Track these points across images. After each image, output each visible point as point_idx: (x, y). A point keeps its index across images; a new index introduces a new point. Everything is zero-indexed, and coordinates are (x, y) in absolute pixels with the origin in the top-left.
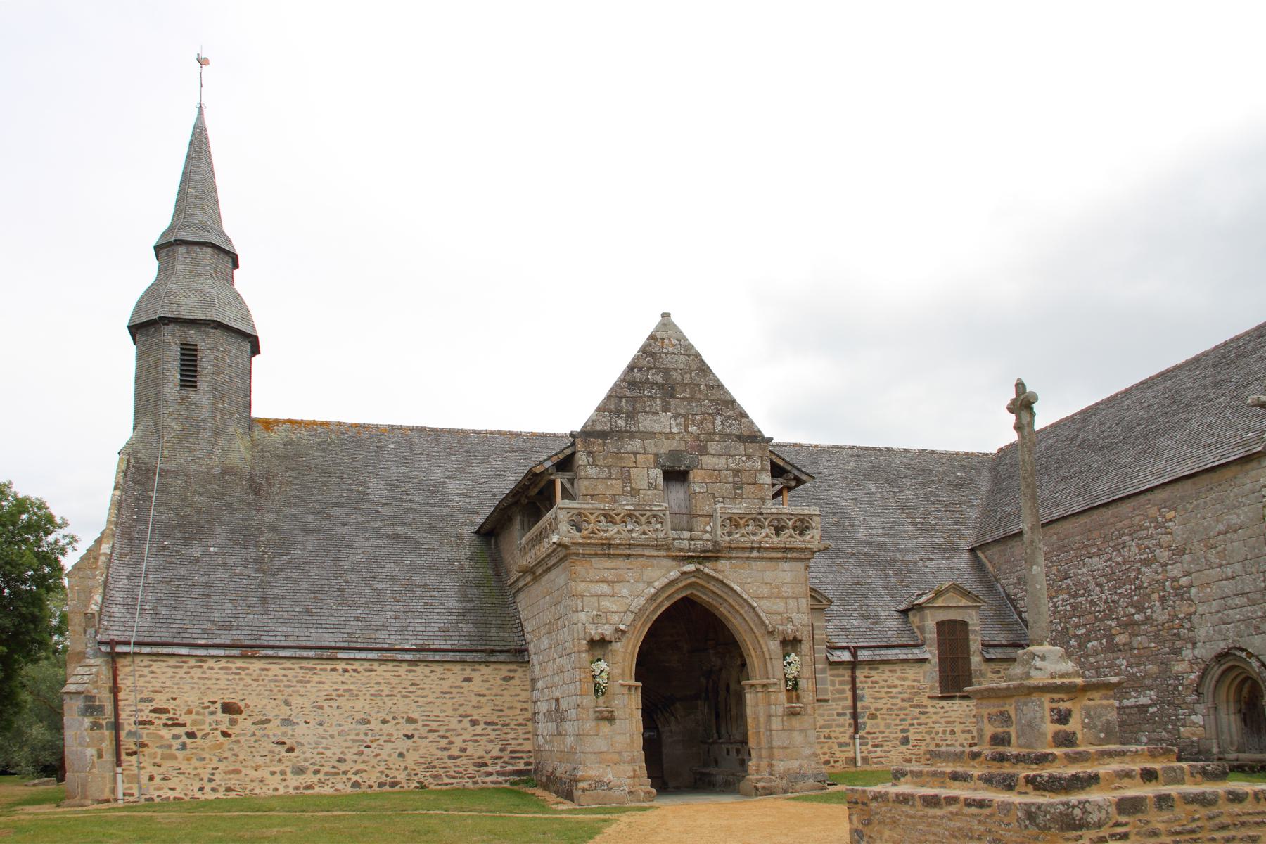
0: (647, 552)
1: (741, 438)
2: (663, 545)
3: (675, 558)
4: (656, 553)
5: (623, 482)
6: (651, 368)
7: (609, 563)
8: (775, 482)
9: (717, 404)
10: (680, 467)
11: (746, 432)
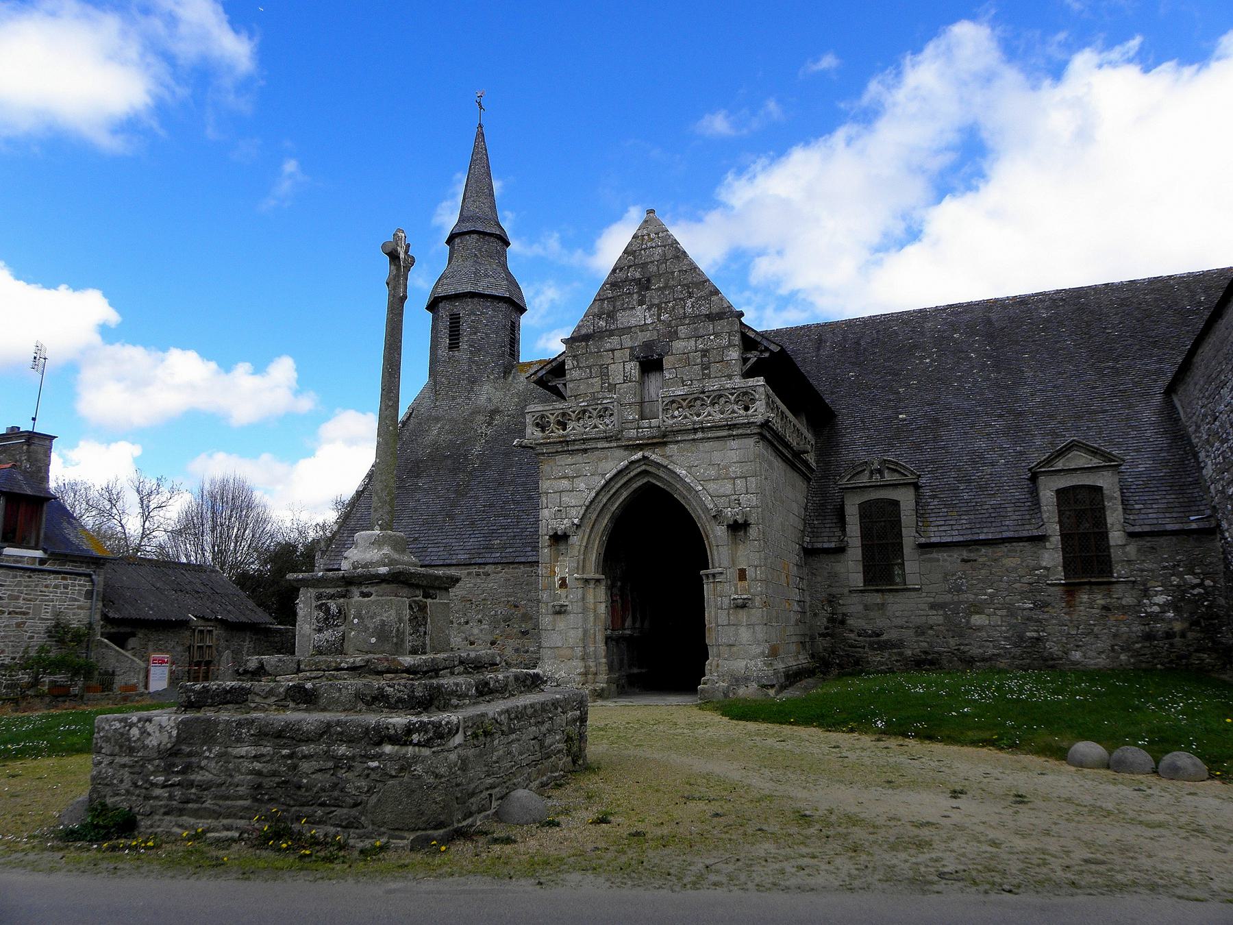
0: (599, 446)
1: (711, 317)
2: (612, 437)
3: (627, 447)
4: (607, 445)
5: (602, 379)
6: (629, 267)
7: (570, 460)
8: (749, 356)
9: (689, 287)
10: (652, 356)
11: (715, 310)
